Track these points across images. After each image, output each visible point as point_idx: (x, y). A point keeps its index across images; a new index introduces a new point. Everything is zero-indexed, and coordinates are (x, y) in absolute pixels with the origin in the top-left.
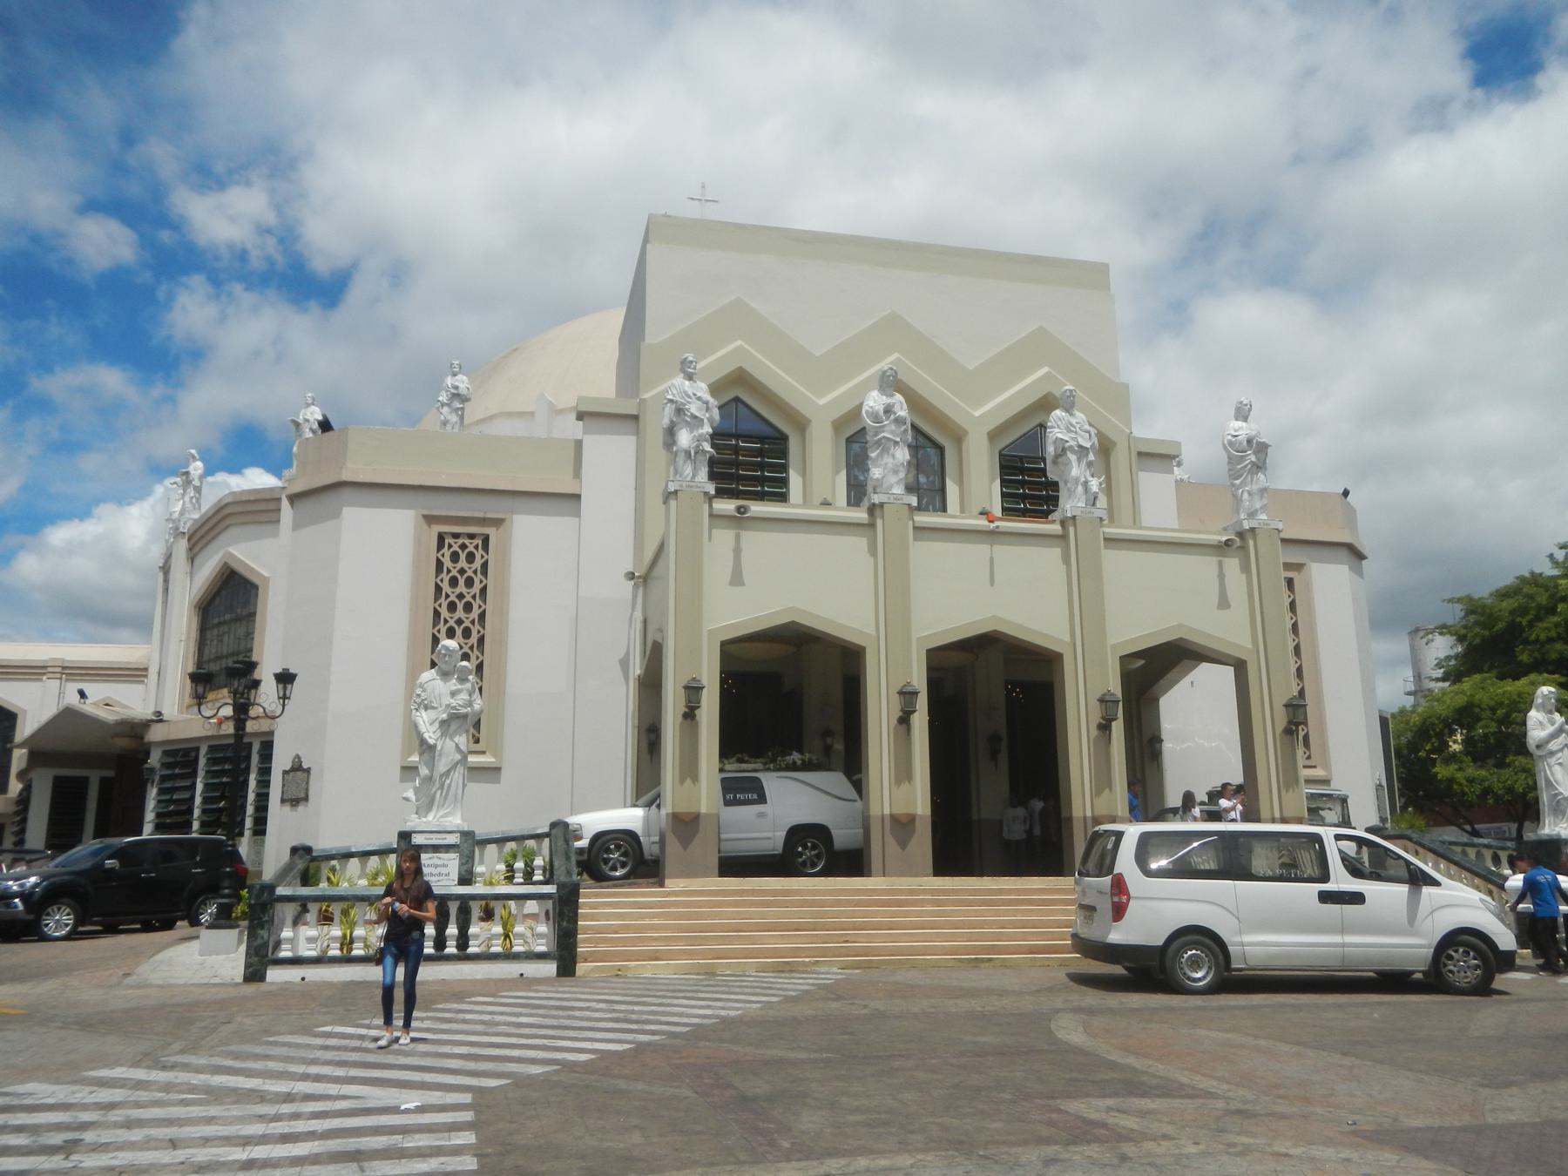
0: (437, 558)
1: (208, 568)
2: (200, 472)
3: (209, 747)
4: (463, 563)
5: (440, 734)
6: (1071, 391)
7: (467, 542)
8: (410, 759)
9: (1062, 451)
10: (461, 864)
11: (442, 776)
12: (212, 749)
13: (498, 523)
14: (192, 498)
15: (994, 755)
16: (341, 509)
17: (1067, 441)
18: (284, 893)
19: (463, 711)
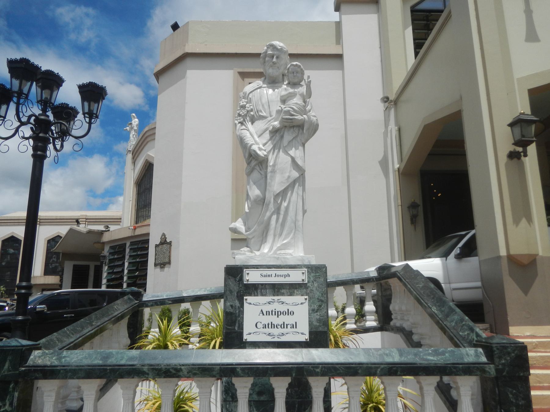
1: (140, 163)
2: (137, 123)
3: (131, 242)
5: (272, 146)
10: (312, 311)
11: (277, 196)
12: (132, 244)
14: (133, 135)
16: (185, 73)
18: (40, 362)
19: (299, 117)
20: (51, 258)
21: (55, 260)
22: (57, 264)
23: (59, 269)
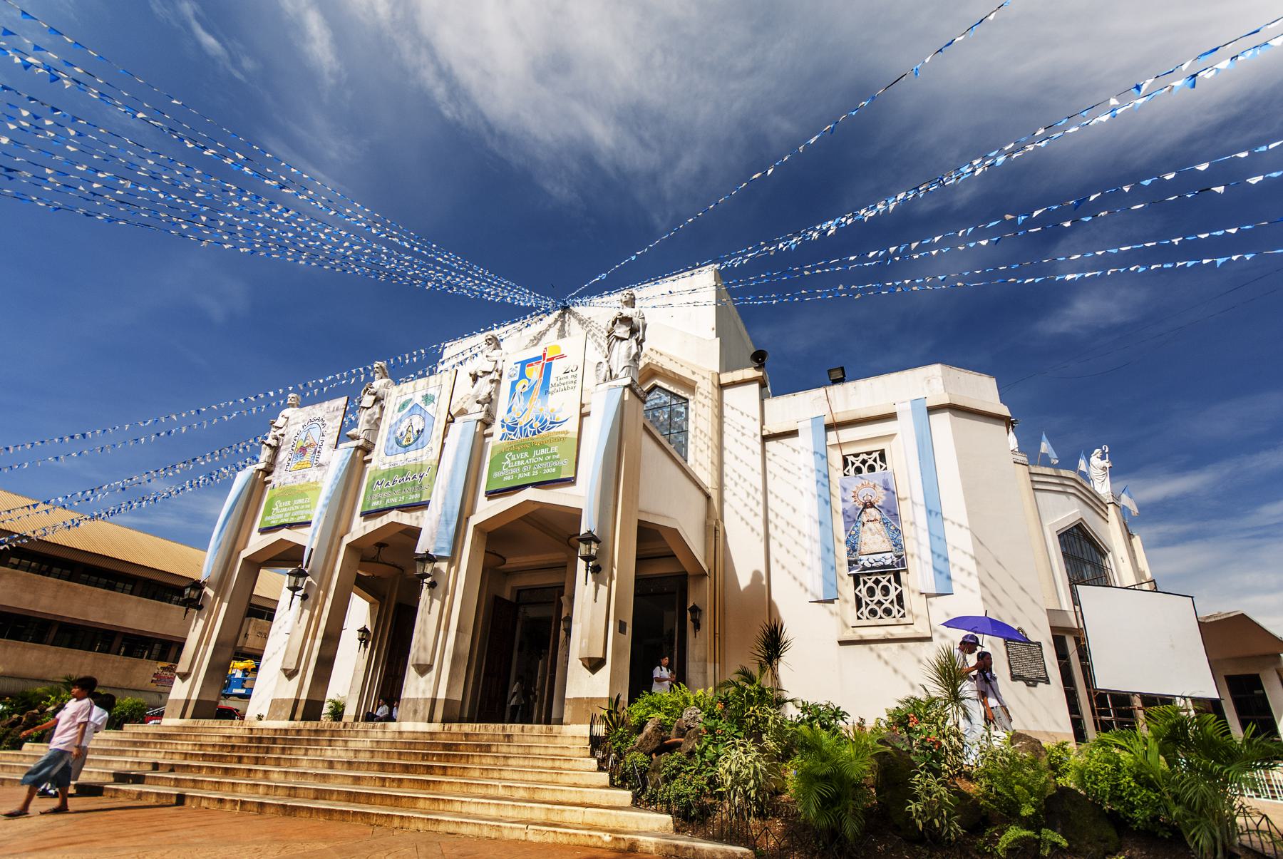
7: (865, 457)
13: (891, 436)
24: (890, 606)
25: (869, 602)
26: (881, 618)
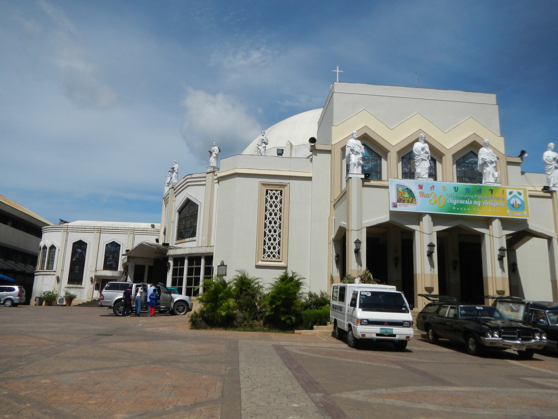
0: (266, 198)
4: (274, 199)
6: (487, 141)
7: (275, 192)
8: (258, 263)
9: (485, 164)
15: (455, 268)
17: (486, 159)
20: (109, 257)
21: (111, 258)
22: (113, 263)
23: (114, 266)
24: (275, 254)
25: (268, 252)
26: (271, 258)
